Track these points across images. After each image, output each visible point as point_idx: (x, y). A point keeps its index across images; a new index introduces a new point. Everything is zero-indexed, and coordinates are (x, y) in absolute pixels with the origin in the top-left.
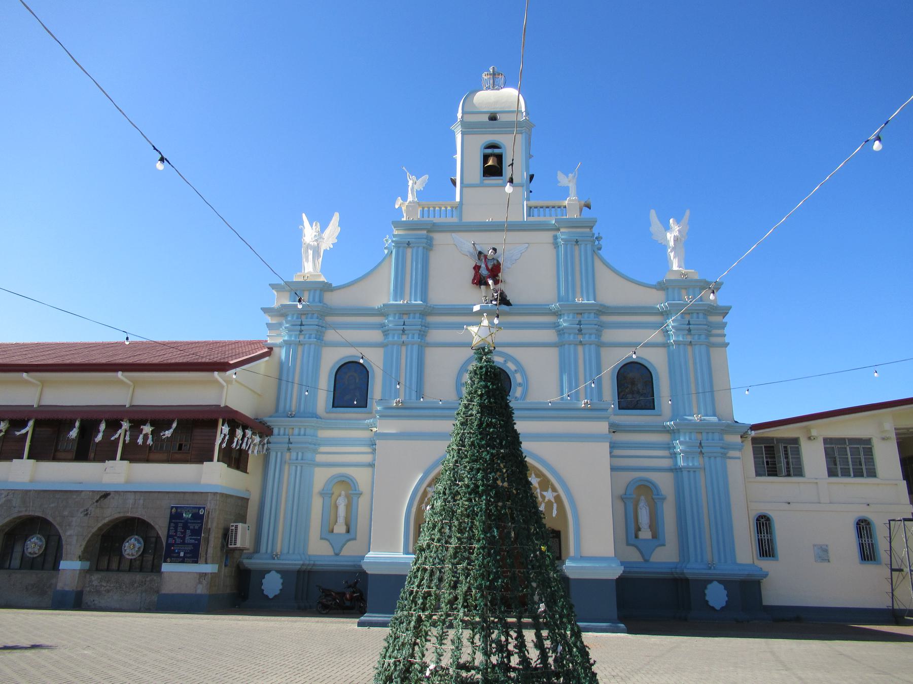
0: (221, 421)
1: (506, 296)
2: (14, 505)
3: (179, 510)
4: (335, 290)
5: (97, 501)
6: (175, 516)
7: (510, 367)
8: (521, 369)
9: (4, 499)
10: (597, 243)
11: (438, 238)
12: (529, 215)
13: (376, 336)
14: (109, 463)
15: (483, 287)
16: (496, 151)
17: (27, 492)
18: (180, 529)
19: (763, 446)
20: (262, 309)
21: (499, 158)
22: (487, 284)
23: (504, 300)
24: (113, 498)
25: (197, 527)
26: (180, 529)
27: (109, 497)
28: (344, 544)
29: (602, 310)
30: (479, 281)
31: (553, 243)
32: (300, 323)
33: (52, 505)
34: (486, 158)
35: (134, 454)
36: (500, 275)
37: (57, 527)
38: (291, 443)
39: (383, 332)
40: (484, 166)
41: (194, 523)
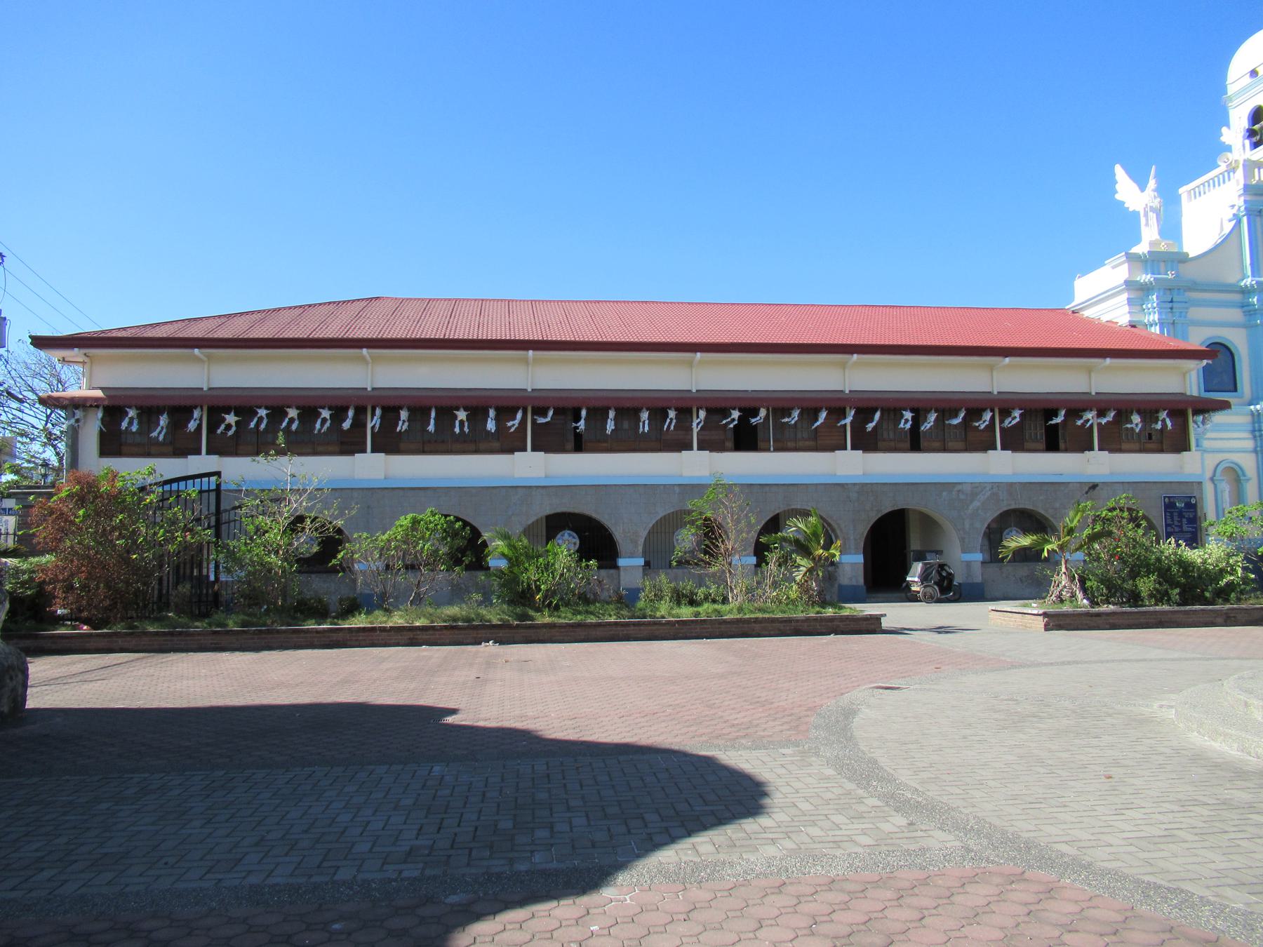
0: (1190, 412)
2: (1001, 498)
3: (1172, 500)
5: (1087, 493)
6: (1169, 506)
9: (990, 492)
13: (1236, 315)
17: (1011, 484)
18: (1176, 518)
24: (1102, 489)
25: (1191, 516)
26: (1176, 518)
27: (1098, 488)
32: (1170, 300)
33: (1041, 498)
35: (1114, 440)
37: (1052, 519)
41: (1189, 512)
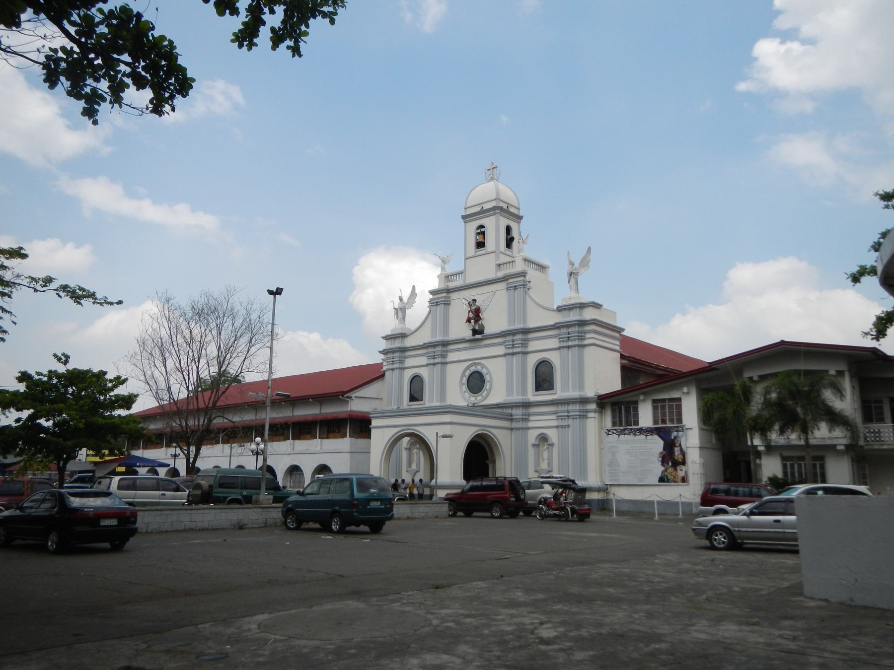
7: (484, 371)
11: (454, 296)
14: (315, 440)
16: (483, 230)
19: (616, 407)
21: (483, 233)
29: (526, 331)
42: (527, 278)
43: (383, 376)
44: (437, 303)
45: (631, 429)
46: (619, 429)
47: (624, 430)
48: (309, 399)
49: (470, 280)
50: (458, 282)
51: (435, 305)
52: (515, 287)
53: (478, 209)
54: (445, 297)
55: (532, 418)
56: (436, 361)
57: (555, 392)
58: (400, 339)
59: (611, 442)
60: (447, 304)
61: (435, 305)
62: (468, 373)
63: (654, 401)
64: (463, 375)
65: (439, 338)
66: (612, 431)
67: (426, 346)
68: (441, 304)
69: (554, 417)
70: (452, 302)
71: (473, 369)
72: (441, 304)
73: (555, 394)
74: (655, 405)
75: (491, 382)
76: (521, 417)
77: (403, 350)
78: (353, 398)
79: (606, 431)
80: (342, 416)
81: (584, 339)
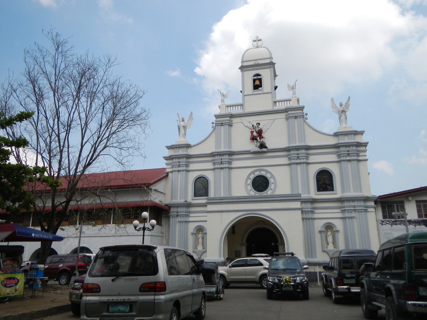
1: (266, 144)
4: (192, 147)
7: (268, 176)
8: (273, 176)
10: (305, 116)
12: (273, 106)
15: (255, 141)
16: (259, 77)
19: (386, 205)
20: (164, 157)
21: (260, 80)
22: (256, 139)
23: (263, 146)
28: (202, 254)
29: (308, 148)
30: (253, 138)
31: (286, 118)
34: (254, 81)
36: (262, 134)
38: (178, 213)
39: (213, 163)
40: (253, 84)
42: (305, 111)
43: (167, 176)
44: (222, 124)
45: (401, 221)
46: (391, 221)
47: (396, 221)
48: (108, 189)
49: (248, 110)
50: (237, 111)
51: (220, 125)
52: (296, 117)
53: (252, 63)
54: (229, 120)
55: (316, 211)
56: (224, 166)
57: (336, 193)
58: (185, 148)
59: (386, 230)
60: (230, 125)
61: (220, 125)
62: (252, 177)
63: (417, 202)
64: (248, 177)
65: (223, 149)
66: (385, 222)
67: (212, 155)
68: (226, 125)
69: (339, 211)
70: (233, 125)
71: (257, 173)
72: (226, 125)
73: (336, 194)
74: (418, 204)
75: (275, 183)
76: (310, 210)
77: (188, 157)
78: (153, 190)
79: (381, 222)
80: (145, 204)
81: (359, 156)
